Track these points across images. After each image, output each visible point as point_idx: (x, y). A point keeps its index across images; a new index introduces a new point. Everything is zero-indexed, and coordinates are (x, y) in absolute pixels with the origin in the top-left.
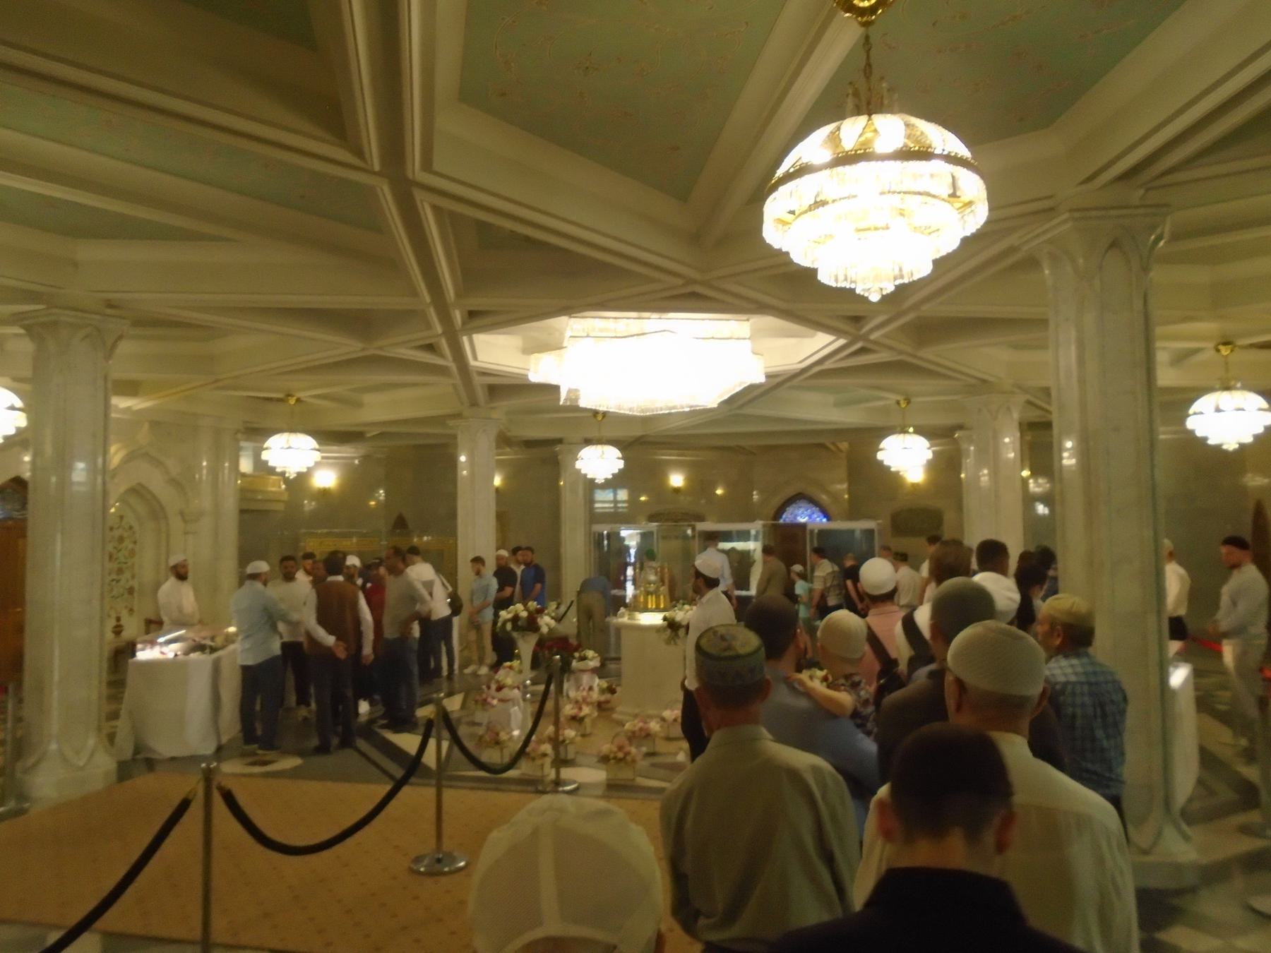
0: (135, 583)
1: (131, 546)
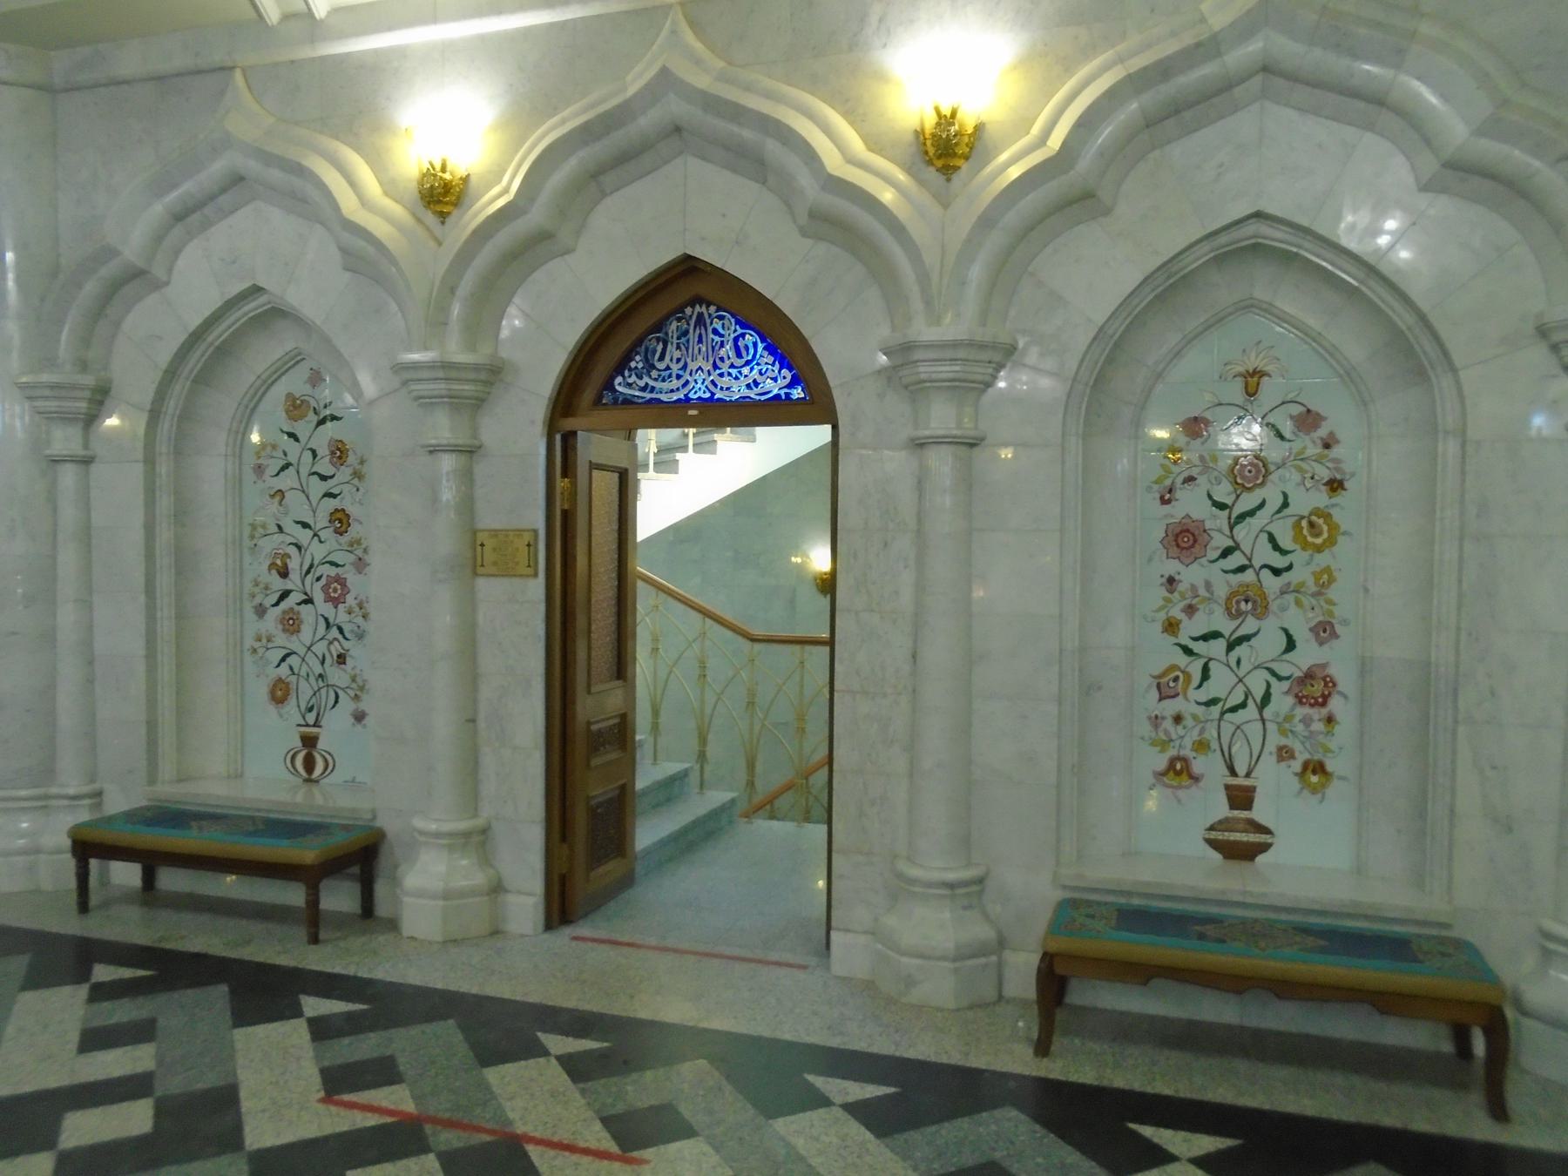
0: (1339, 660)
1: (1307, 500)
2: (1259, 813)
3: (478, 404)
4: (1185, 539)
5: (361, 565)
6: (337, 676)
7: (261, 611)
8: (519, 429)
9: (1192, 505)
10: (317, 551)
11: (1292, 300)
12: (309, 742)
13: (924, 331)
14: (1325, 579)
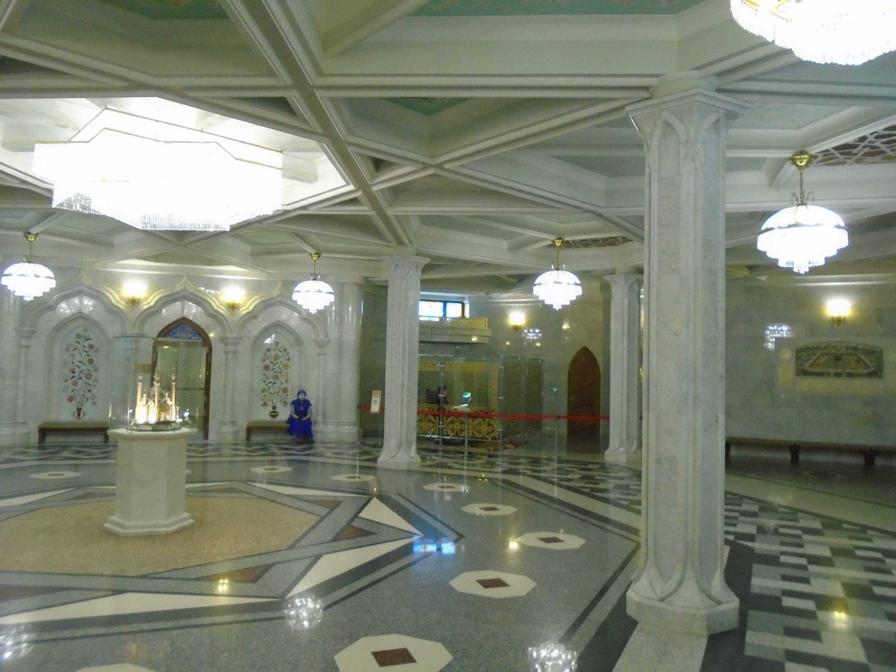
1: (285, 362)
2: (277, 410)
3: (30, 337)
4: (266, 368)
5: (96, 371)
6: (88, 395)
7: (66, 381)
8: (147, 345)
9: (268, 362)
10: (84, 368)
11: (283, 332)
12: (79, 410)
13: (229, 335)
14: (287, 374)
